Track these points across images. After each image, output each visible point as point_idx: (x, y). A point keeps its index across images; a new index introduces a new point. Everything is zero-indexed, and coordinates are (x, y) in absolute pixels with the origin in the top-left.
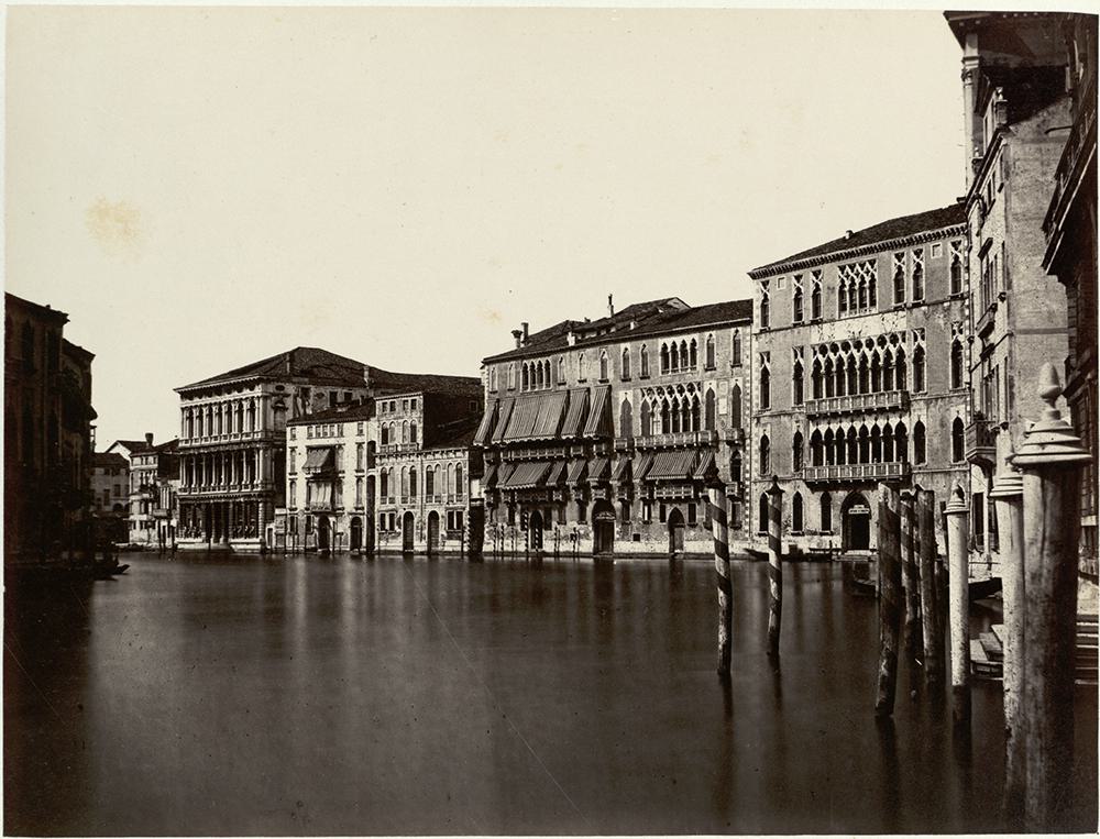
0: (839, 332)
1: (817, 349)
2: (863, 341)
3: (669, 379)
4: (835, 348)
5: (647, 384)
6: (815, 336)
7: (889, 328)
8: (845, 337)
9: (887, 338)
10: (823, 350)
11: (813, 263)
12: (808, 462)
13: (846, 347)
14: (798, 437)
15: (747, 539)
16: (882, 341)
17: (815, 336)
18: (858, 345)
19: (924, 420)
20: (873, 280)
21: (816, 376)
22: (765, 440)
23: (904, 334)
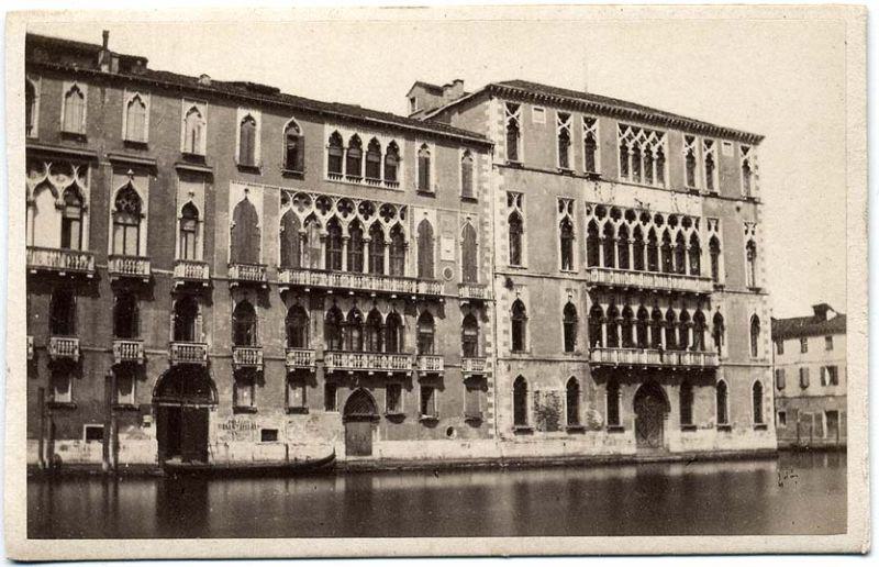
0: (625, 195)
1: (594, 207)
2: (653, 215)
3: (340, 188)
4: (616, 213)
5: (294, 186)
6: (590, 193)
7: (684, 210)
8: (631, 204)
9: (680, 219)
10: (600, 211)
11: (591, 109)
12: (582, 342)
13: (630, 215)
14: (570, 310)
15: (492, 437)
16: (673, 221)
17: (590, 193)
18: (645, 218)
19: (723, 313)
20: (660, 153)
21: (593, 242)
22: (518, 307)
23: (698, 220)
